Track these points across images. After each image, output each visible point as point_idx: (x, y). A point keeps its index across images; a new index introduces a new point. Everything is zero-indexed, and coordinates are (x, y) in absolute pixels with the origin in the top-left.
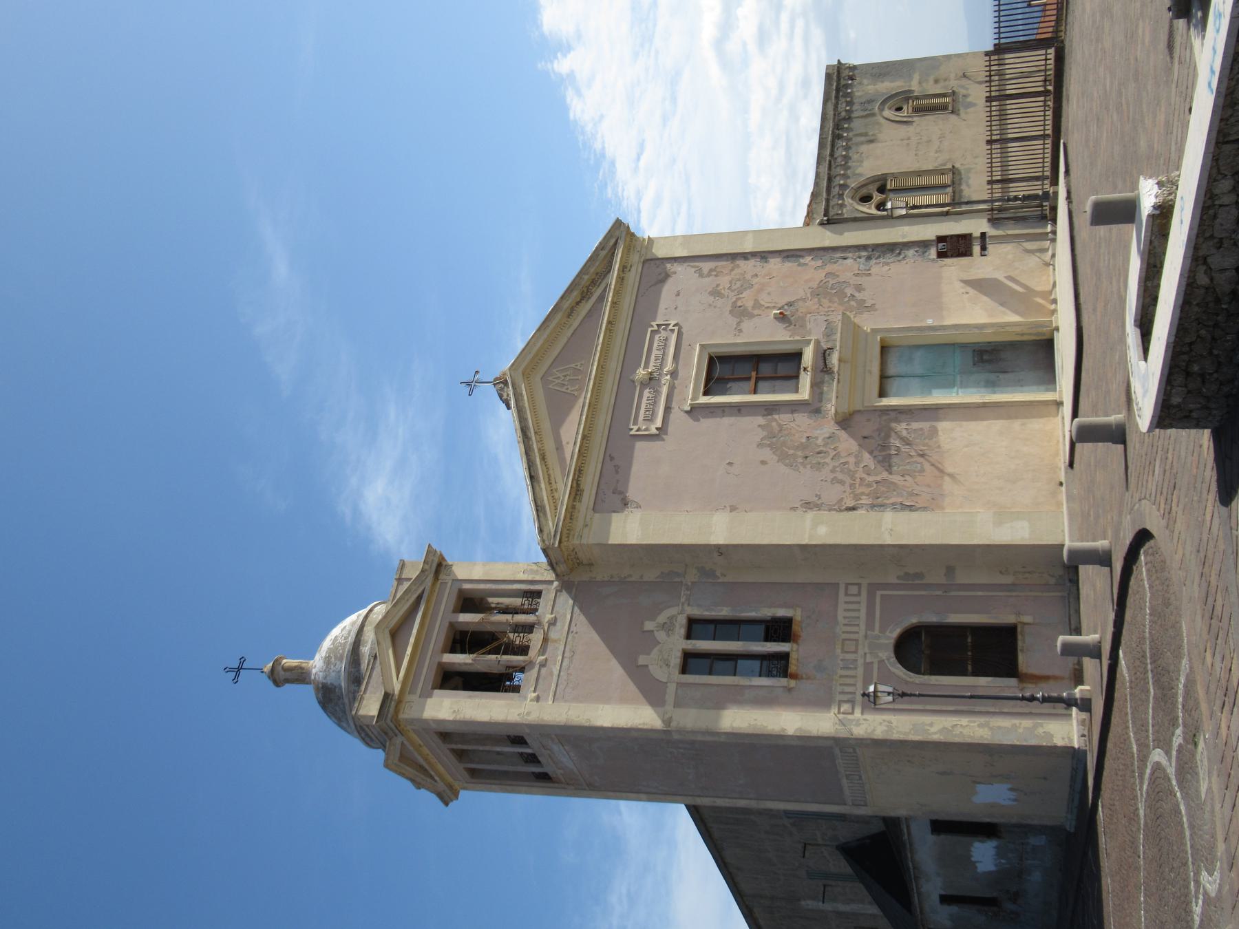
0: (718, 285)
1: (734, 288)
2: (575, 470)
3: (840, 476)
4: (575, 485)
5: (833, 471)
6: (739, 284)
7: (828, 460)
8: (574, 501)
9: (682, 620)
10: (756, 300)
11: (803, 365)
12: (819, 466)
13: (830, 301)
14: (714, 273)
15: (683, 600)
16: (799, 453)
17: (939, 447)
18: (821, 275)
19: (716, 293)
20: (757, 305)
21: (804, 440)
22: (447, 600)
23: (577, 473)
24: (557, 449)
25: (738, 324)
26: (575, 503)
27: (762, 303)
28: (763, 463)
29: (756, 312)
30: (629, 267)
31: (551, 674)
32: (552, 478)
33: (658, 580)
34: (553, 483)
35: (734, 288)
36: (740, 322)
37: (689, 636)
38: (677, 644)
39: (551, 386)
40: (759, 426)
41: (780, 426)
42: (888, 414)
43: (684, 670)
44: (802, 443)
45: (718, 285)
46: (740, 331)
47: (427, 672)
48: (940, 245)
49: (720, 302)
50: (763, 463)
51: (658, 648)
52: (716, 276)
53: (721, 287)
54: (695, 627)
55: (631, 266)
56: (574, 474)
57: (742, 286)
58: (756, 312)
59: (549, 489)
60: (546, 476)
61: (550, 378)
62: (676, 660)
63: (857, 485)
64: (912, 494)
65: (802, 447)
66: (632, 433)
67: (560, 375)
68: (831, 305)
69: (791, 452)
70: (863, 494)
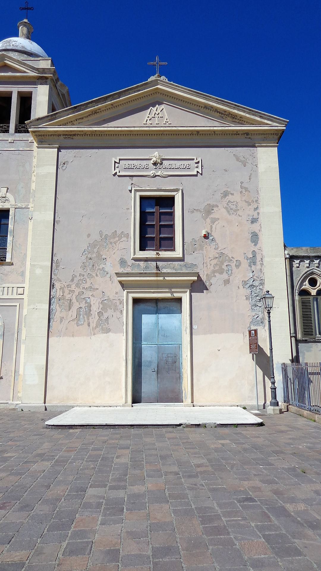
2: (82, 131)
3: (76, 280)
4: (74, 133)
5: (80, 275)
6: (234, 207)
7: (89, 271)
8: (63, 135)
10: (219, 219)
11: (160, 253)
12: (84, 267)
13: (216, 264)
14: (244, 190)
16: (94, 255)
17: (94, 334)
18: (241, 259)
20: (214, 221)
21: (104, 257)
23: (82, 133)
24: (104, 120)
26: (62, 136)
27: (217, 222)
28: (89, 235)
29: (208, 220)
30: (248, 137)
33: (32, 190)
34: (78, 121)
35: (230, 204)
36: (200, 211)
41: (115, 243)
42: (120, 304)
44: (102, 256)
45: (232, 194)
46: (192, 212)
48: (253, 332)
50: (89, 235)
52: (241, 192)
53: (230, 195)
55: (249, 138)
56: (80, 131)
59: (72, 120)
60: (81, 117)
63: (69, 289)
64: (62, 319)
65: (99, 256)
68: (212, 265)
69: (95, 250)
70: (63, 292)
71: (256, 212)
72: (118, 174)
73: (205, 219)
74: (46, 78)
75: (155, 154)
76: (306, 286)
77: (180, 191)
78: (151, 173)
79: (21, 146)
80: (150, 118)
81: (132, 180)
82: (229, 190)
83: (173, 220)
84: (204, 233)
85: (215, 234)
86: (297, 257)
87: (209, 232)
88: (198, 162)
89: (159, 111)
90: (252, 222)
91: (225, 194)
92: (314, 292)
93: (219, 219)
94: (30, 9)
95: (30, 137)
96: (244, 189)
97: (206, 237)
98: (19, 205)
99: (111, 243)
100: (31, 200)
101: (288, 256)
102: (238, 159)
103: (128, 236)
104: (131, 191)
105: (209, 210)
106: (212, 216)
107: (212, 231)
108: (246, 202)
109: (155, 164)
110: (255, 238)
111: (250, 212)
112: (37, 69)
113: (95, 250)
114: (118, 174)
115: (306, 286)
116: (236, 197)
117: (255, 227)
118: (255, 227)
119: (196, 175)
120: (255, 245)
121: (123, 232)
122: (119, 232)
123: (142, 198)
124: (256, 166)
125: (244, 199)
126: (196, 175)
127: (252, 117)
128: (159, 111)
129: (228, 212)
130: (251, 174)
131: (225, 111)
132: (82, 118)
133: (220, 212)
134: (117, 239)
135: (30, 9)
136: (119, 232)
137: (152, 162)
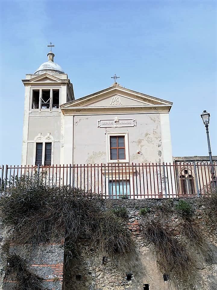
0: (150, 134)
1: (149, 139)
9: (50, 141)
11: (119, 160)
19: (147, 135)
20: (142, 146)
22: (56, 88)
25: (136, 142)
28: (88, 154)
29: (140, 146)
31: (37, 115)
32: (83, 104)
35: (149, 139)
38: (44, 141)
40: (100, 152)
43: (37, 144)
45: (150, 134)
47: (36, 88)
49: (144, 135)
50: (88, 154)
53: (149, 135)
54: (48, 144)
57: (149, 141)
58: (140, 146)
62: (39, 141)
71: (160, 142)
72: (100, 127)
73: (138, 145)
74: (65, 83)
75: (116, 118)
76: (183, 173)
77: (127, 133)
78: (115, 126)
79: (55, 114)
81: (106, 129)
82: (148, 132)
83: (124, 146)
84: (138, 151)
85: (142, 152)
86: (178, 161)
87: (140, 151)
88: (135, 121)
89: (117, 98)
90: (159, 146)
91: (147, 135)
93: (144, 145)
94: (53, 46)
95: (59, 110)
96: (155, 133)
97: (138, 153)
98: (56, 141)
99: (98, 157)
100: (61, 138)
101: (174, 161)
102: (151, 119)
103: (105, 153)
104: (106, 134)
105: (140, 142)
106: (141, 144)
107: (141, 150)
108: (156, 138)
109: (116, 122)
110: (160, 153)
111: (157, 142)
112: (62, 80)
113: (92, 160)
114: (100, 127)
116: (151, 136)
117: (160, 149)
118: (160, 149)
119: (134, 127)
120: (160, 156)
121: (103, 152)
122: (101, 152)
123: (111, 137)
125: (155, 136)
126: (134, 127)
127: (157, 101)
128: (117, 98)
129: (148, 142)
130: (158, 126)
131: (146, 99)
132: (84, 103)
133: (144, 142)
134: (101, 155)
135: (53, 46)
136: (101, 152)
137: (114, 121)
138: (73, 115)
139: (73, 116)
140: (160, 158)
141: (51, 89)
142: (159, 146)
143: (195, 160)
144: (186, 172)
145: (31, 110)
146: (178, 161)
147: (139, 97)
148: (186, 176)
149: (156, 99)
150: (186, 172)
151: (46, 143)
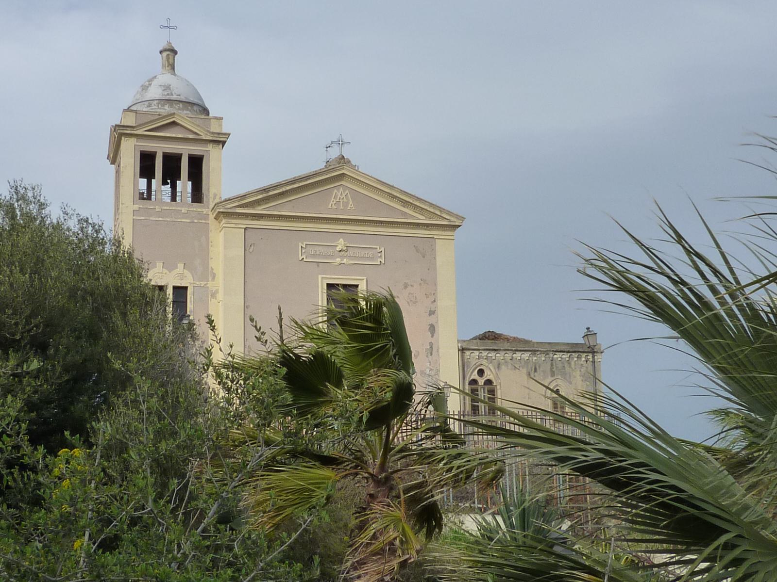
15: (197, 283)
22: (196, 149)
37: (175, 288)
39: (335, 191)
47: (149, 146)
51: (168, 272)
52: (420, 284)
54: (180, 292)
61: (341, 190)
66: (300, 245)
67: (344, 195)
72: (305, 260)
76: (475, 376)
77: (365, 281)
80: (335, 202)
90: (430, 315)
92: (481, 381)
102: (417, 251)
110: (432, 329)
112: (213, 133)
114: (305, 260)
115: (475, 376)
117: (432, 320)
118: (432, 320)
124: (435, 258)
135: (172, 28)
138: (245, 226)
139: (243, 230)
140: (432, 340)
141: (186, 150)
142: (430, 315)
143: (500, 350)
144: (481, 372)
145: (137, 204)
146: (469, 349)
147: (395, 197)
148: (481, 381)
149: (431, 205)
150: (481, 372)
151: (175, 288)
